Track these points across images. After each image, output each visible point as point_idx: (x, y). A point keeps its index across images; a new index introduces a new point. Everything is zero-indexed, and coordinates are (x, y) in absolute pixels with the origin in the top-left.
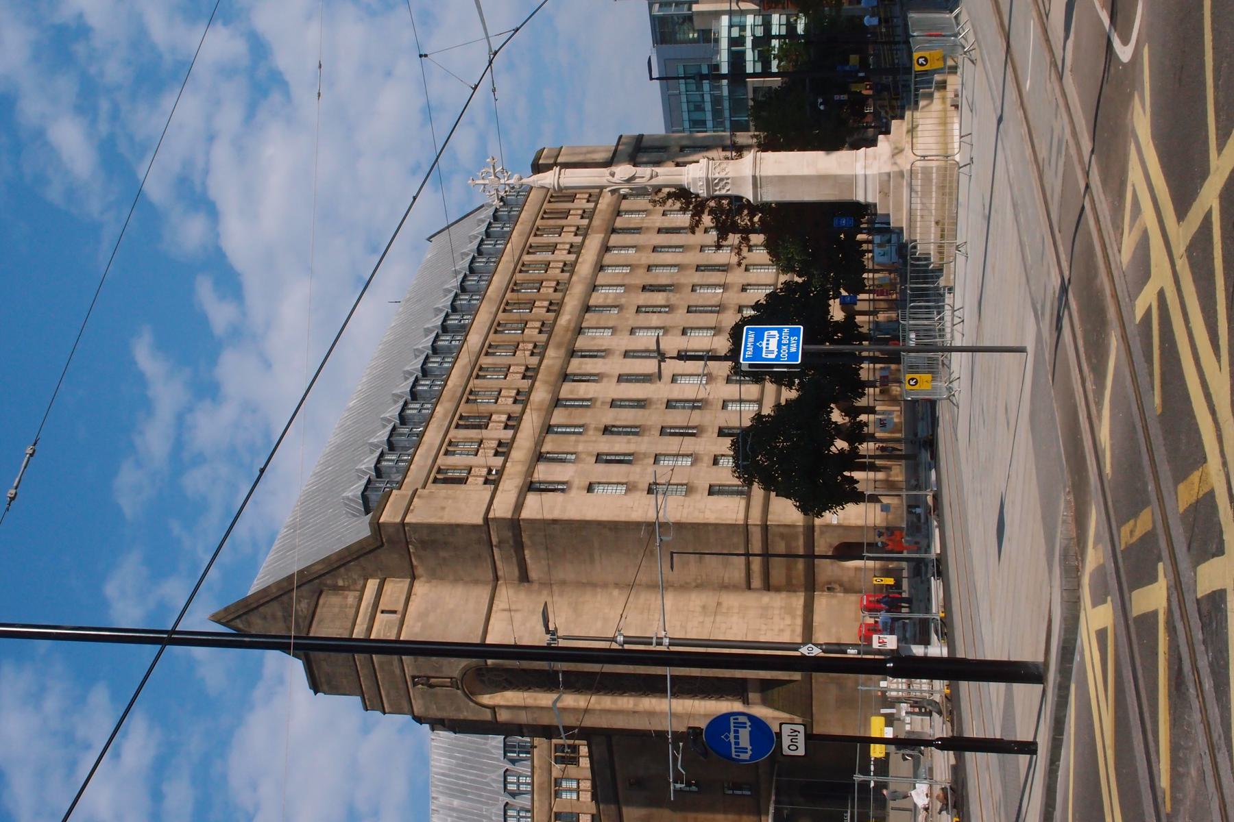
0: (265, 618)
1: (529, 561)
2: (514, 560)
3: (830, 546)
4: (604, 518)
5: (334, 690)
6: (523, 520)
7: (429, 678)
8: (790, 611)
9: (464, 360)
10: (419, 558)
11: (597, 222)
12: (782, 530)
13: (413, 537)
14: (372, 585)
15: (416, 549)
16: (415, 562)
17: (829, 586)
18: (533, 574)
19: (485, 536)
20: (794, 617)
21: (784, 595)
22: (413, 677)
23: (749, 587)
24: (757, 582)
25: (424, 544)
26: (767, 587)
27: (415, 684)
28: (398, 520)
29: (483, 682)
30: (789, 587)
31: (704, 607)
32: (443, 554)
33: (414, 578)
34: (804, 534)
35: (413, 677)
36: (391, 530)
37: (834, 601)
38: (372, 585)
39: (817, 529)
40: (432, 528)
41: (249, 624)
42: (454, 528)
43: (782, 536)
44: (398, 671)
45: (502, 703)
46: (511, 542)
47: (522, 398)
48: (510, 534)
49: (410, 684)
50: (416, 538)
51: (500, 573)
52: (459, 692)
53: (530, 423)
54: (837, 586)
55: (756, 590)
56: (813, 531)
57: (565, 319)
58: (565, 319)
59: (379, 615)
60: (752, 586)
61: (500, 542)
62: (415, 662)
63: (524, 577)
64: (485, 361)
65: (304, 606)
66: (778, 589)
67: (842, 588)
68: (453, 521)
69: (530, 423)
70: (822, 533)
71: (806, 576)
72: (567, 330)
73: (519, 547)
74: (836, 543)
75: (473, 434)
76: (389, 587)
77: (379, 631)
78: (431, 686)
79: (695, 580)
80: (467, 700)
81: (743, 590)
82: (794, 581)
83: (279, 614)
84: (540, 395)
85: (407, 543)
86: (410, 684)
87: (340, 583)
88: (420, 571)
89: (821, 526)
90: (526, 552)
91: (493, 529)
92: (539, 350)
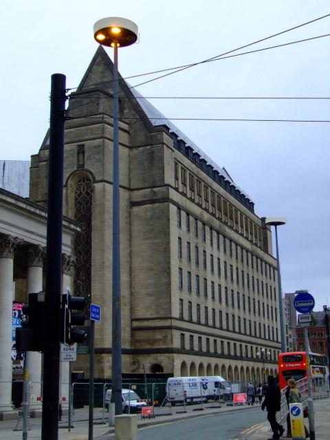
0: (102, 72)
1: (144, 206)
2: (145, 199)
3: (161, 362)
4: (171, 246)
6: (168, 205)
7: (83, 153)
10: (144, 151)
11: (254, 247)
12: (170, 336)
13: (156, 148)
16: (140, 149)
18: (135, 209)
19: (158, 184)
21: (130, 339)
22: (83, 145)
23: (132, 320)
24: (136, 324)
27: (78, 146)
28: (164, 141)
29: (80, 181)
32: (146, 164)
33: (130, 148)
35: (83, 145)
36: (159, 137)
37: (129, 365)
39: (171, 355)
41: (99, 64)
43: (165, 337)
44: (87, 137)
45: (69, 191)
49: (79, 143)
51: (135, 192)
52: (75, 169)
54: (136, 366)
55: (131, 324)
56: (169, 353)
60: (133, 322)
61: (154, 192)
63: (133, 204)
64: (209, 189)
66: (132, 335)
70: (169, 357)
71: (141, 350)
72: (224, 231)
73: (152, 201)
74: (162, 365)
76: (126, 135)
77: (108, 128)
78: (78, 154)
79: (136, 292)
80: (70, 172)
81: (131, 317)
82: (138, 344)
83: (106, 80)
85: (151, 145)
86: (79, 143)
87: (126, 111)
88: (135, 151)
89: (173, 357)
90: (149, 205)
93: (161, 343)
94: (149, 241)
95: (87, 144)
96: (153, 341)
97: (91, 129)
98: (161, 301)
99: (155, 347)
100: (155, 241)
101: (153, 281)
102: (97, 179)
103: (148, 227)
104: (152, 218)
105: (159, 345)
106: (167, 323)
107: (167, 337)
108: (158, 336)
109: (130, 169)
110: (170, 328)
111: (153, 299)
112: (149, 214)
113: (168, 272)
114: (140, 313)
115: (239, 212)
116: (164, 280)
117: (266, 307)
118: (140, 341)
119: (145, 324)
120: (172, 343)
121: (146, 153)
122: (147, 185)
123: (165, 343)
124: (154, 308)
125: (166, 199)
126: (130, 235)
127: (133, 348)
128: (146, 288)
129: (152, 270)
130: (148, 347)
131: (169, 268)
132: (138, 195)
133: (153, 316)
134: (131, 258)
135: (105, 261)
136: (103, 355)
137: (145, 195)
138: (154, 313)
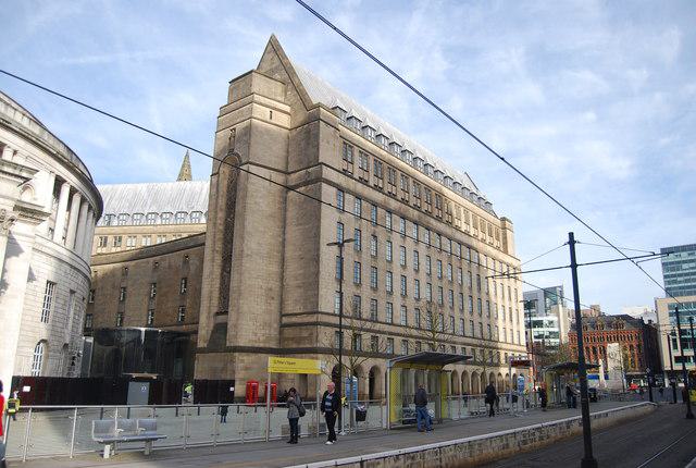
5: (231, 91)
8: (268, 339)
9: (412, 170)
14: (287, 109)
20: (264, 342)
23: (282, 316)
24: (285, 320)
25: (308, 132)
26: (283, 326)
30: (281, 339)
31: (271, 289)
32: (303, 143)
38: (287, 109)
40: (317, 136)
42: (317, 147)
47: (392, 195)
53: (378, 197)
57: (433, 223)
58: (433, 223)
59: (268, 110)
63: (289, 188)
65: (278, 76)
66: (281, 333)
68: (321, 147)
69: (378, 197)
73: (306, 183)
75: (372, 167)
84: (393, 204)
88: (294, 132)
92: (417, 208)
96: (300, 340)
97: (242, 111)
99: (301, 346)
101: (301, 271)
106: (312, 319)
108: (305, 334)
109: (288, 152)
110: (316, 324)
113: (316, 260)
114: (290, 309)
115: (462, 209)
116: (312, 269)
117: (507, 311)
118: (288, 339)
119: (294, 320)
120: (317, 341)
125: (319, 179)
130: (294, 346)
131: (318, 256)
132: (293, 179)
133: (301, 311)
134: (284, 247)
135: (245, 248)
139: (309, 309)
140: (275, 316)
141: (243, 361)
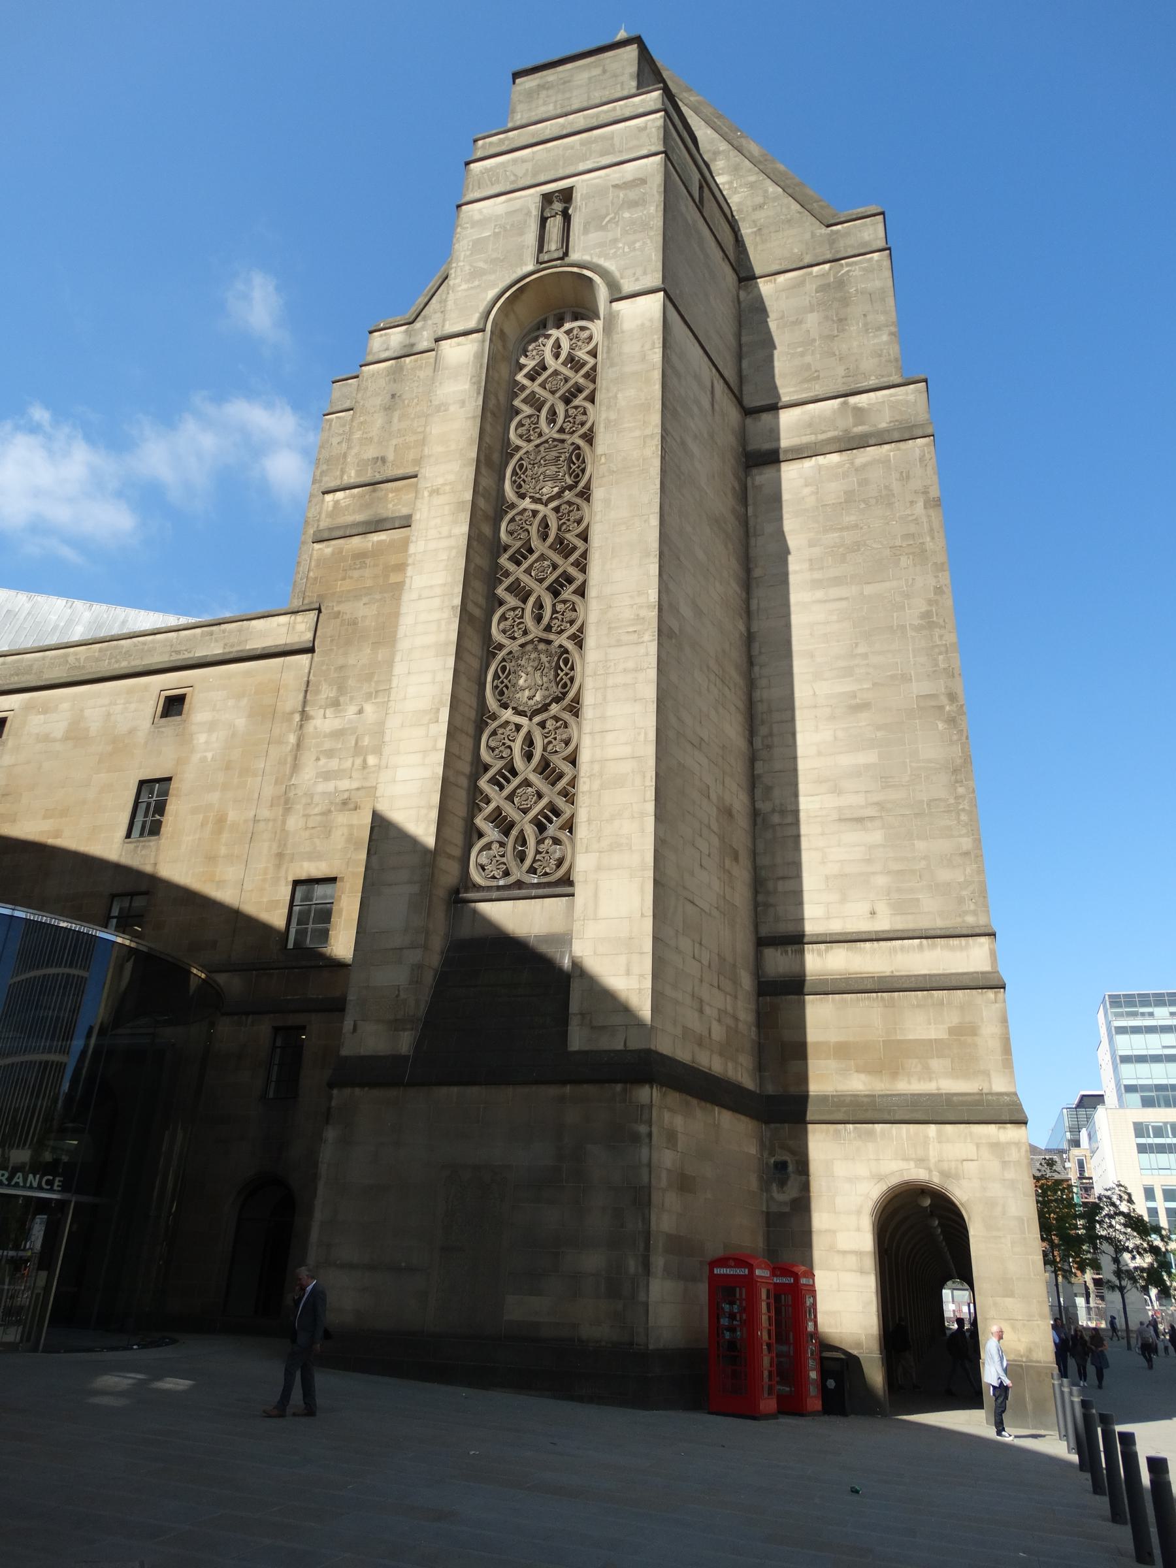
2: (812, 438)
3: (945, 1175)
10: (801, 283)
15: (824, 275)
17: (791, 1168)
34: (981, 1094)
43: (965, 1032)
44: (582, 167)
46: (860, 429)
48: (883, 425)
50: (851, 274)
62: (615, 186)
67: (787, 1209)
70: (997, 1147)
73: (851, 444)
74: (960, 1194)
81: (756, 927)
90: (835, 458)
91: (891, 395)
93: (935, 1064)
94: (835, 592)
95: (581, 184)
98: (920, 845)
99: (910, 1085)
100: (868, 590)
102: (628, 287)
103: (834, 536)
104: (849, 498)
105: (927, 1073)
107: (973, 1031)
111: (877, 836)
112: (834, 489)
121: (811, 287)
122: (818, 390)
123: (966, 1063)
124: (881, 881)
126: (748, 571)
127: (770, 1089)
128: (837, 791)
129: (865, 706)
133: (883, 924)
136: (644, 1094)
137: (810, 424)
138: (882, 908)
139: (931, 913)
140: (742, 942)
141: (671, 1137)
